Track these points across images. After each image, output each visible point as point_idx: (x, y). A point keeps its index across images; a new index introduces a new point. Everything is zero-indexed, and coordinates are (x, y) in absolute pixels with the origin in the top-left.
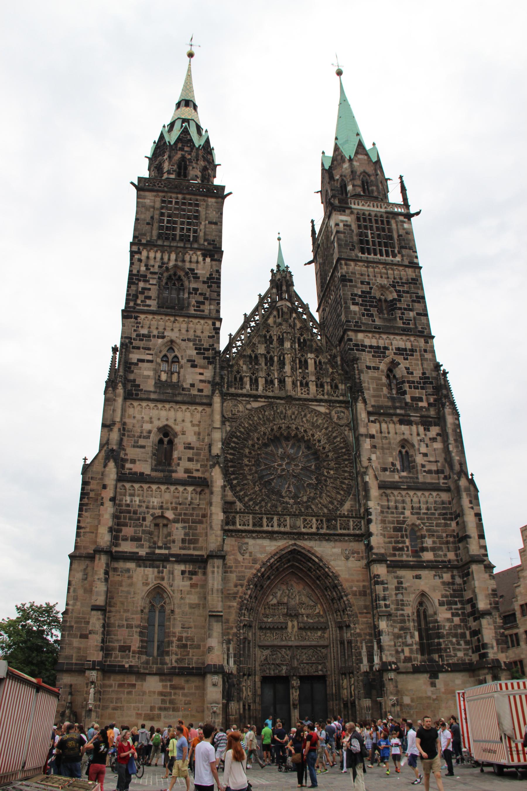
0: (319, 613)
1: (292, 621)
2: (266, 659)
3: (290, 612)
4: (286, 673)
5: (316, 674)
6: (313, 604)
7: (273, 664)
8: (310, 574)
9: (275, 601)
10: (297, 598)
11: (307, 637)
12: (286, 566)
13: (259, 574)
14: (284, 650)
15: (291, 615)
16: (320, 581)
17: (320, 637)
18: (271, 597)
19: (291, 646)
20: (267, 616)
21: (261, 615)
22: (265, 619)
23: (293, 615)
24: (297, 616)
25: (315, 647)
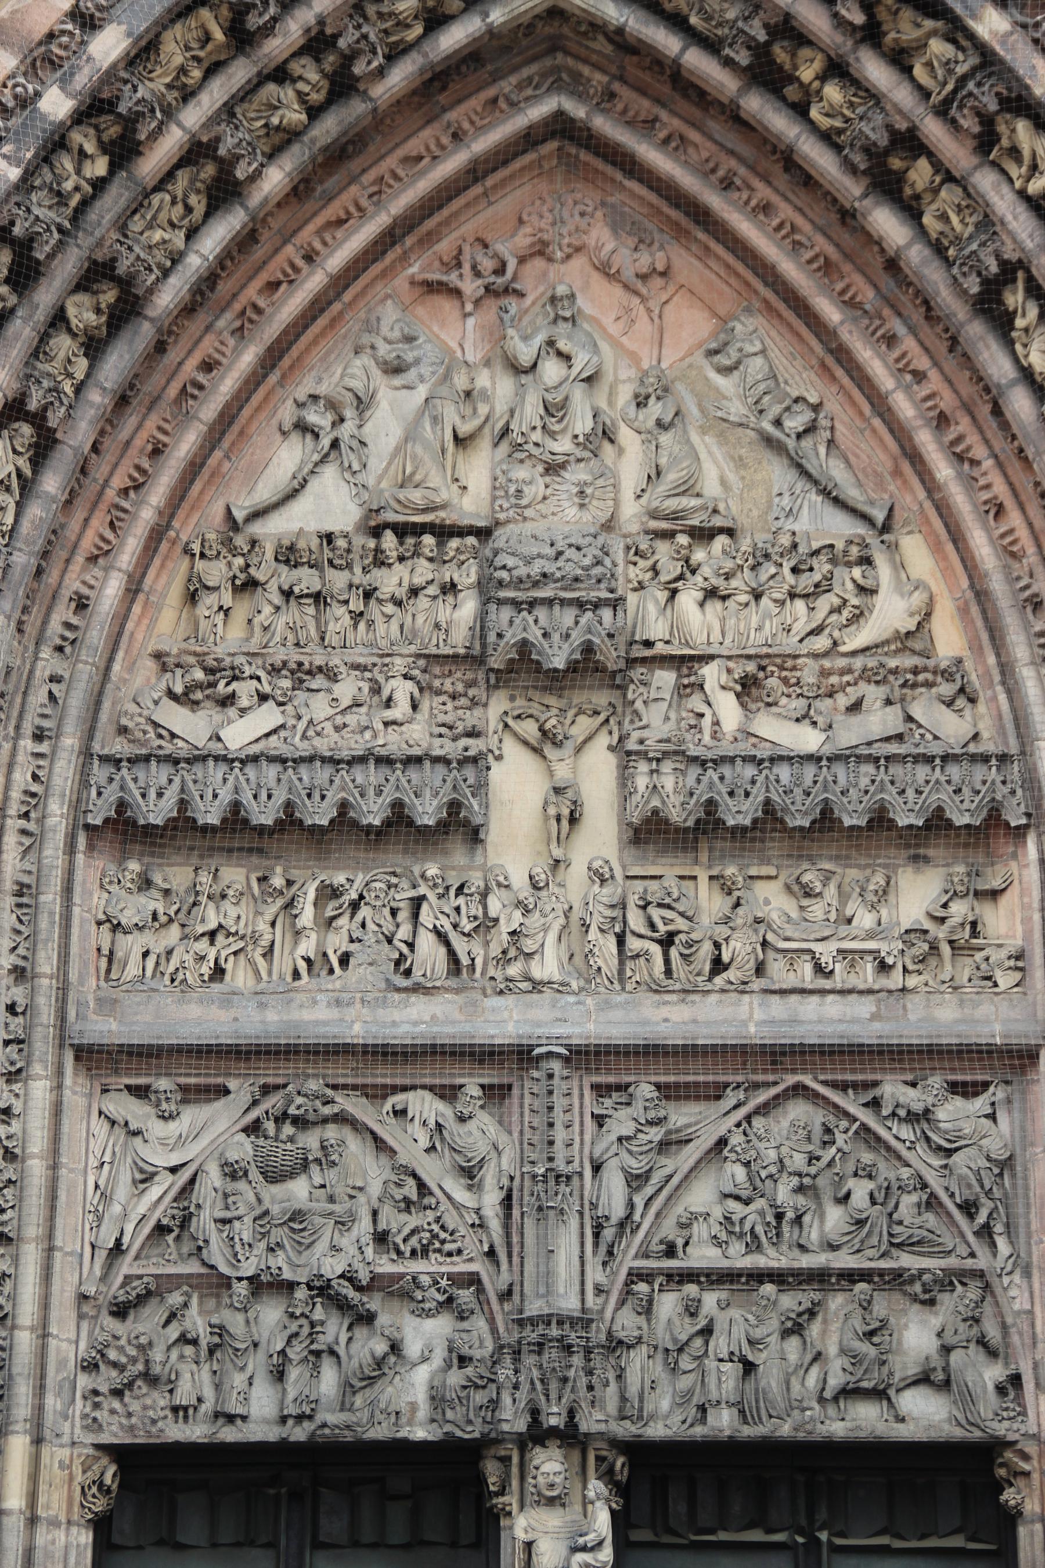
0: (913, 638)
1: (546, 742)
2: (175, 1227)
3: (512, 627)
4: (437, 1399)
5: (865, 1420)
6: (840, 527)
7: (262, 1286)
8: (780, 123)
9: (331, 506)
10: (630, 462)
11: (739, 948)
12: (454, 37)
13: (56, 104)
14: (425, 1106)
15: (524, 669)
16: (911, 210)
17: (925, 946)
18: (289, 457)
19: (524, 1056)
20: (211, 685)
21: (138, 683)
22: (191, 726)
23: (566, 669)
24: (602, 673)
25: (853, 1062)
